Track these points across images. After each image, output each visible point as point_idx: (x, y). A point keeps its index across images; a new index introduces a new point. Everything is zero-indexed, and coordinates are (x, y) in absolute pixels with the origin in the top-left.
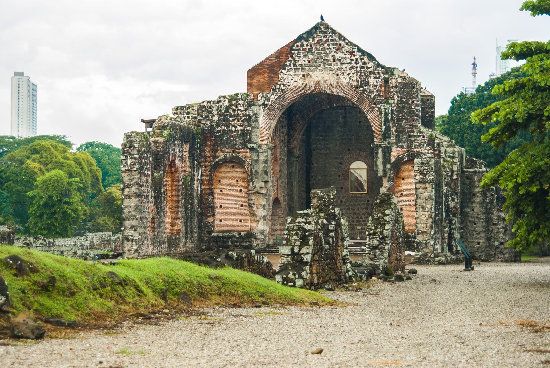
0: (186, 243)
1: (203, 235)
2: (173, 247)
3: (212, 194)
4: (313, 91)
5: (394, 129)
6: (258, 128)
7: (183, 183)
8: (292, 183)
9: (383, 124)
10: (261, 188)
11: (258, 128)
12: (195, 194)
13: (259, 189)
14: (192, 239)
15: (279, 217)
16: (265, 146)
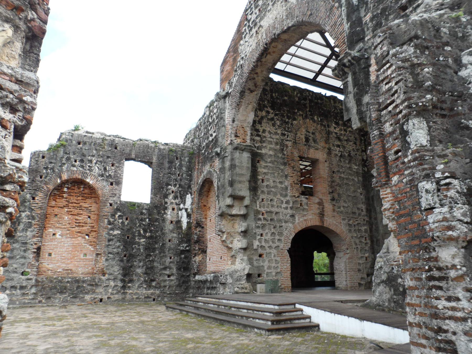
0: (124, 287)
1: (191, 278)
2: (61, 293)
3: (199, 225)
4: (266, 44)
5: (368, 18)
6: (223, 126)
7: (118, 210)
8: (375, 209)
9: (345, 21)
10: (230, 206)
11: (223, 126)
12: (169, 227)
13: (224, 209)
14: (154, 284)
15: (345, 254)
16: (230, 146)
